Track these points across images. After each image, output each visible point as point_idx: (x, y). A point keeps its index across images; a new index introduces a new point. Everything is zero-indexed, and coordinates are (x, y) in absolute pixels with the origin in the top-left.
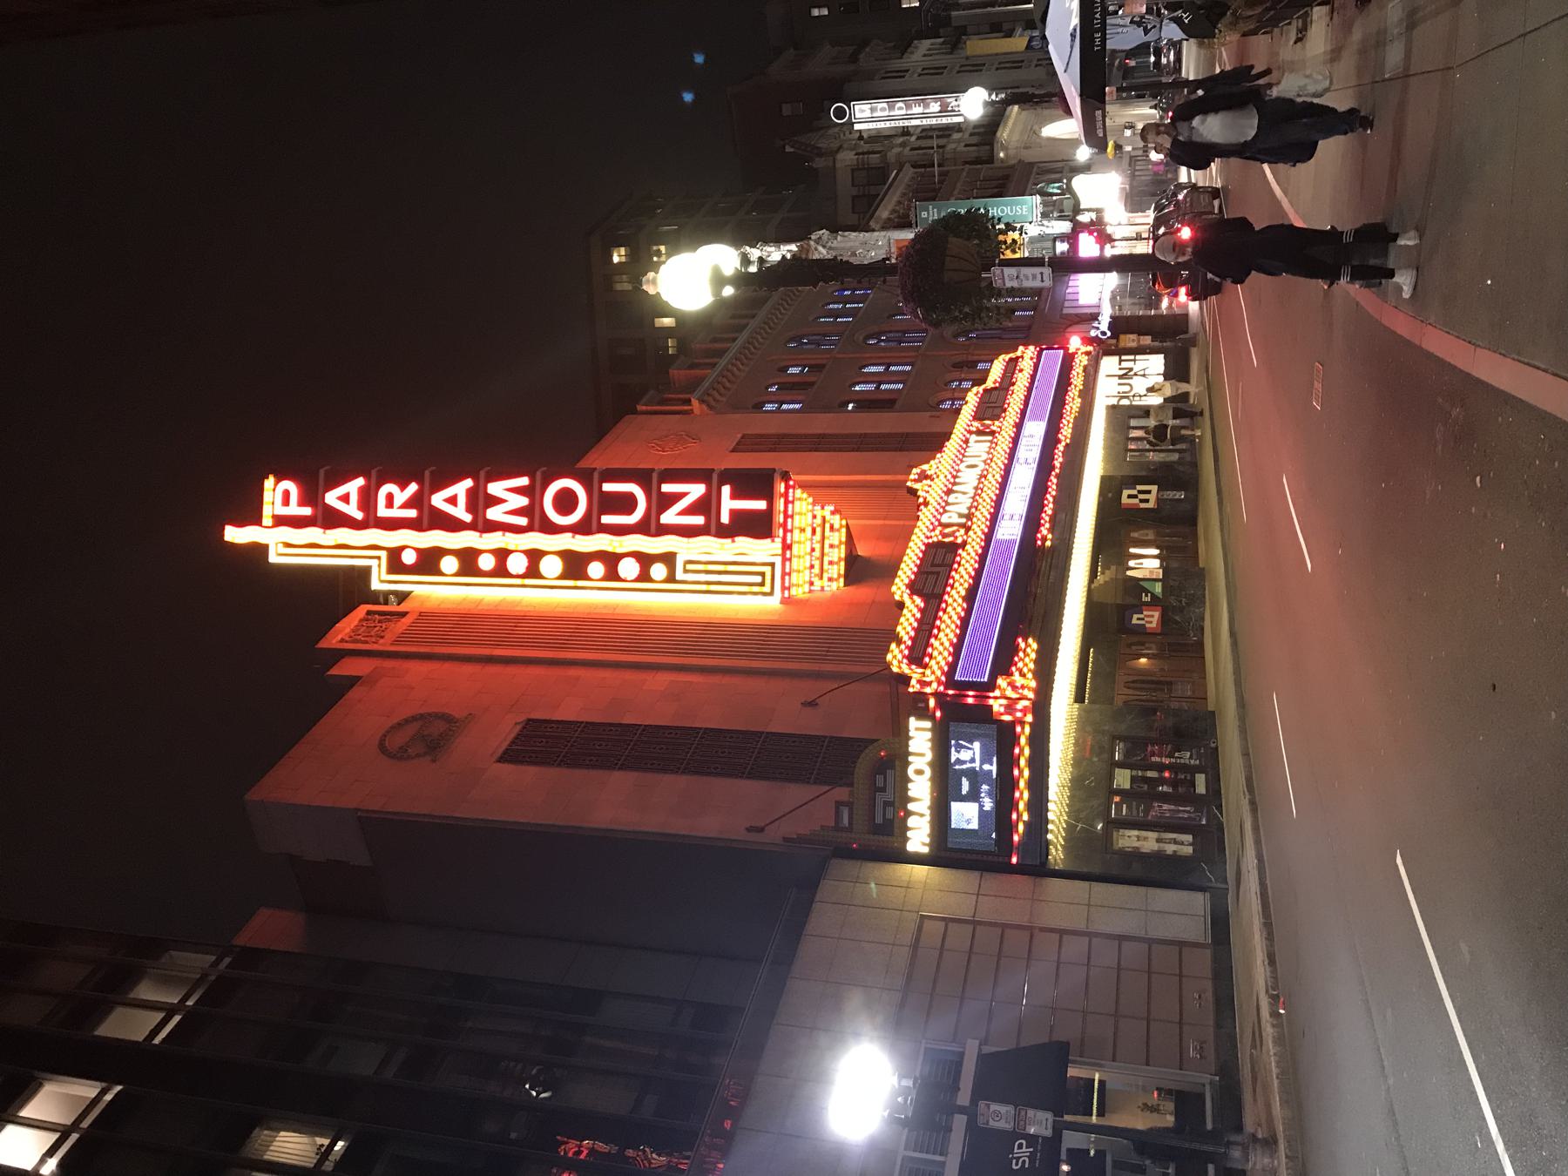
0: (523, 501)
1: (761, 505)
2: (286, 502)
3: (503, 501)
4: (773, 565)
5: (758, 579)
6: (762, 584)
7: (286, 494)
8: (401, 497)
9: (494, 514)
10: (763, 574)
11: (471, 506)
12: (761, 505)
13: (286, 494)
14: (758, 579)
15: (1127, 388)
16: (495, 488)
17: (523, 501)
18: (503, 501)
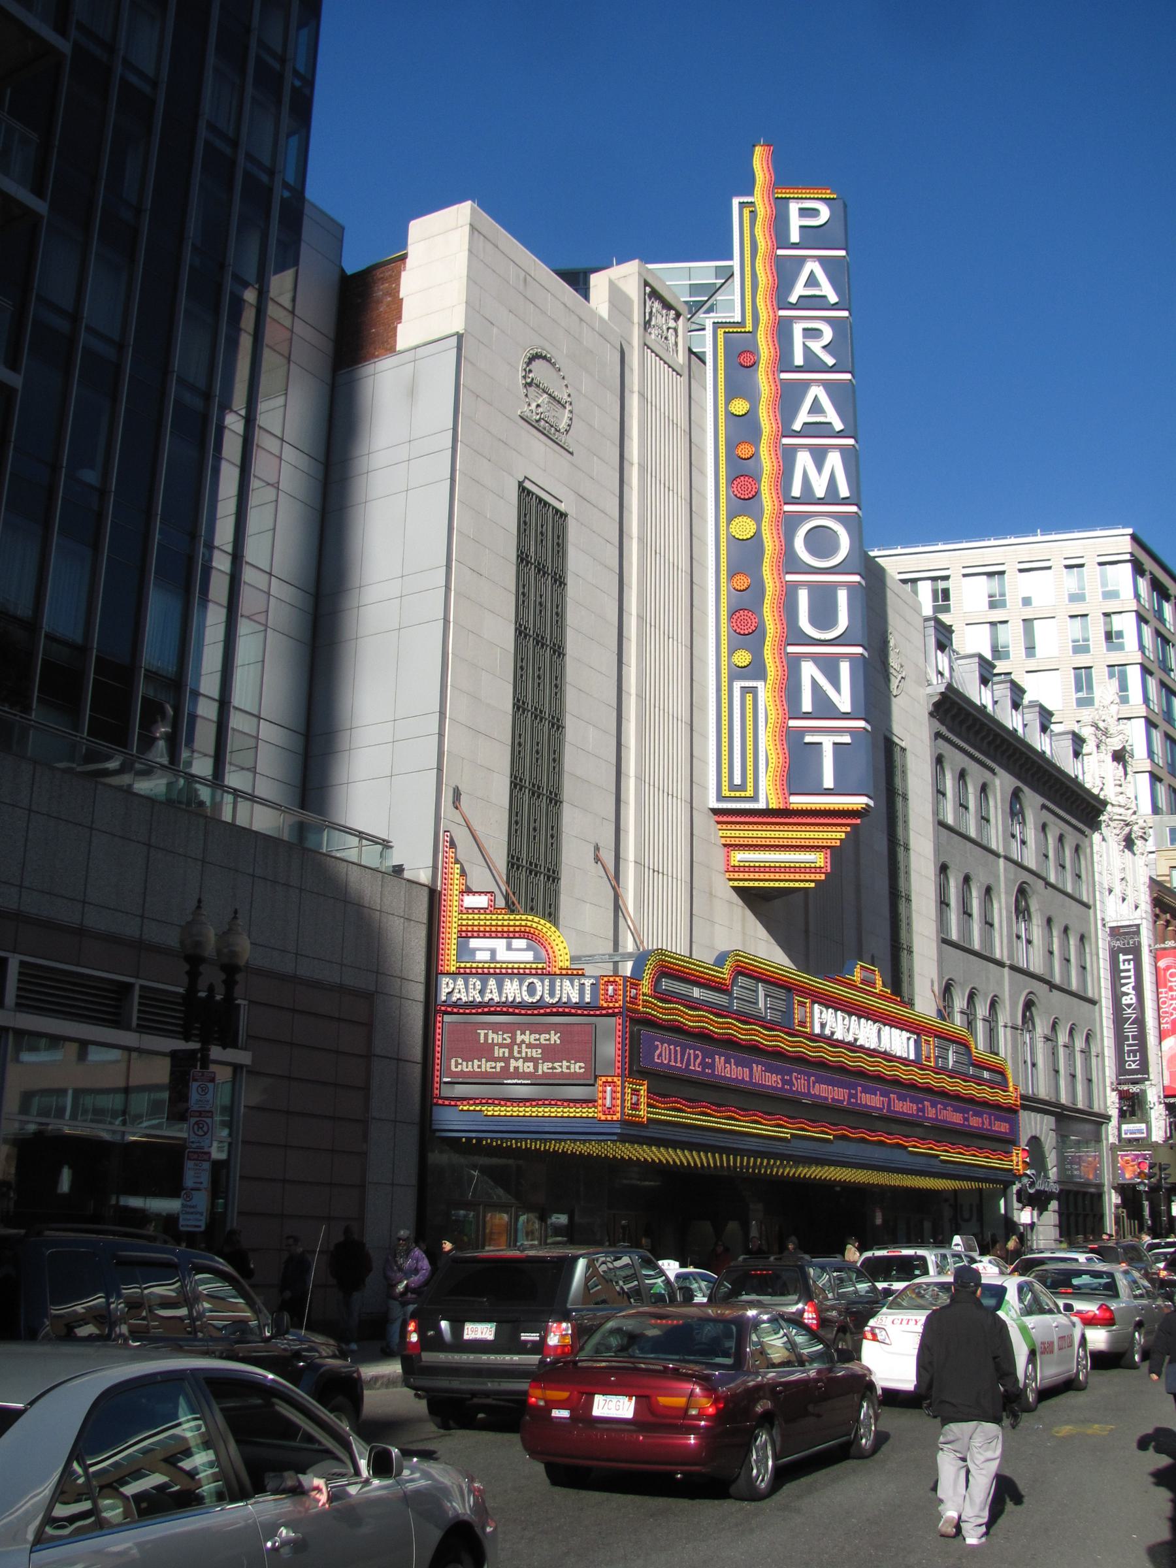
0: (820, 491)
1: (828, 782)
2: (804, 212)
3: (819, 466)
4: (755, 798)
5: (737, 780)
6: (733, 787)
7: (814, 213)
8: (816, 346)
9: (804, 460)
10: (742, 787)
11: (811, 430)
12: (828, 782)
13: (814, 213)
14: (737, 780)
15: (966, 1215)
16: (834, 460)
17: (820, 491)
18: (819, 466)
